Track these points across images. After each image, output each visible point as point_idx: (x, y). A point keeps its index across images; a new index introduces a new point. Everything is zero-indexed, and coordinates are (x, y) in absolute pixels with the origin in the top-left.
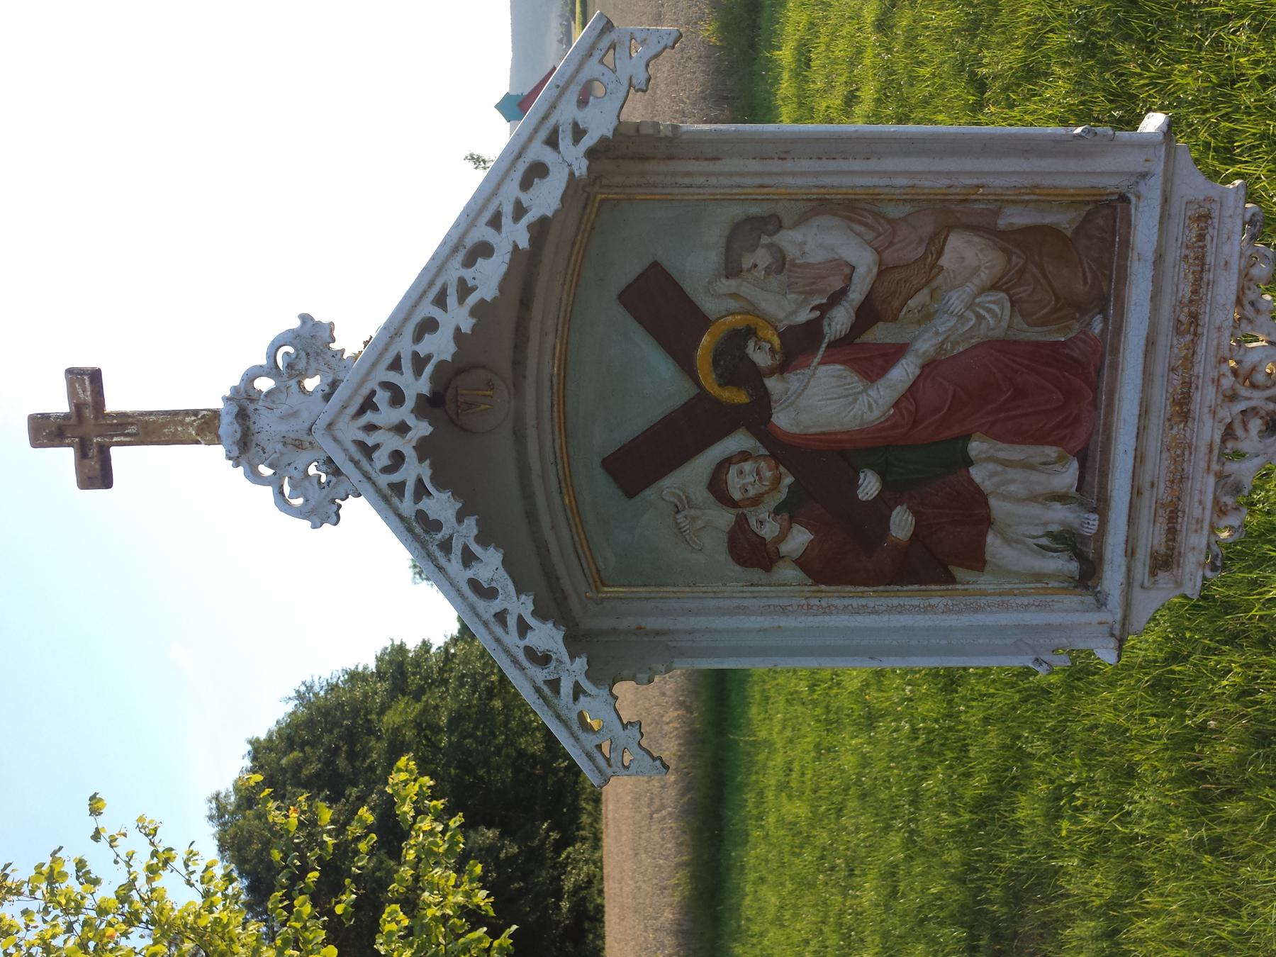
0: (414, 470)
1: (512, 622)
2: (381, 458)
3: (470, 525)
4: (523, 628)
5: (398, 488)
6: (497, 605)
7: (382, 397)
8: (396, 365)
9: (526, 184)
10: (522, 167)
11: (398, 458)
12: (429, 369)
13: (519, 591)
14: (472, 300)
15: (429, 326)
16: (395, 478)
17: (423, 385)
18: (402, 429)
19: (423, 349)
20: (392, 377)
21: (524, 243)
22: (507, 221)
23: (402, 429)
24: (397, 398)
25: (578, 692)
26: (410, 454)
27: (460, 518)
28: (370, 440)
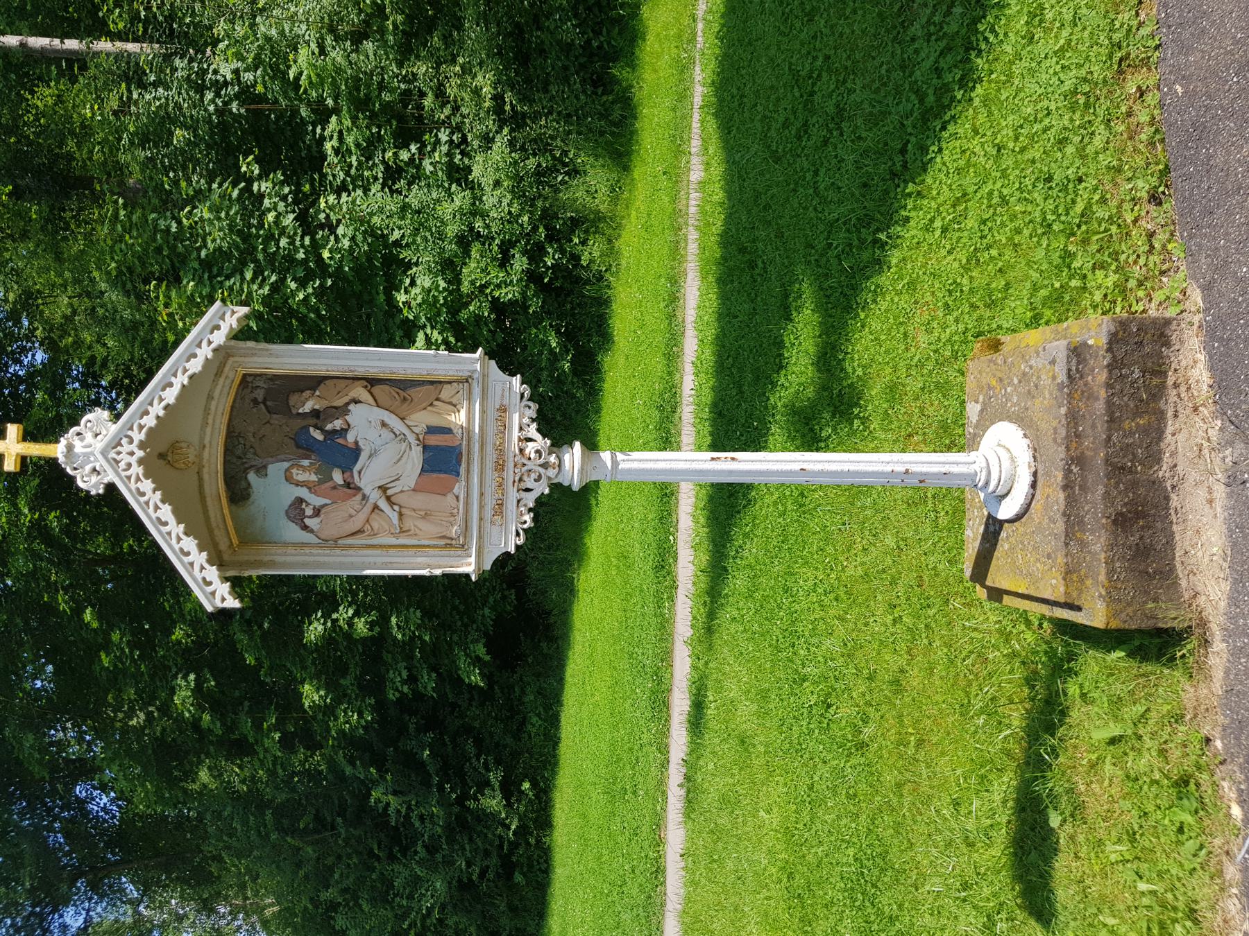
0: (137, 470)
1: (174, 535)
2: (122, 465)
3: (158, 493)
4: (179, 539)
5: (129, 478)
6: (167, 529)
7: (124, 441)
8: (131, 429)
9: (188, 361)
10: (187, 355)
11: (129, 465)
12: (144, 430)
13: (179, 523)
14: (163, 404)
15: (147, 413)
16: (128, 473)
17: (142, 436)
18: (132, 454)
19: (143, 422)
20: (130, 433)
21: (185, 382)
22: (179, 373)
23: (132, 454)
24: (131, 441)
25: (202, 568)
26: (135, 465)
27: (154, 491)
28: (118, 458)
